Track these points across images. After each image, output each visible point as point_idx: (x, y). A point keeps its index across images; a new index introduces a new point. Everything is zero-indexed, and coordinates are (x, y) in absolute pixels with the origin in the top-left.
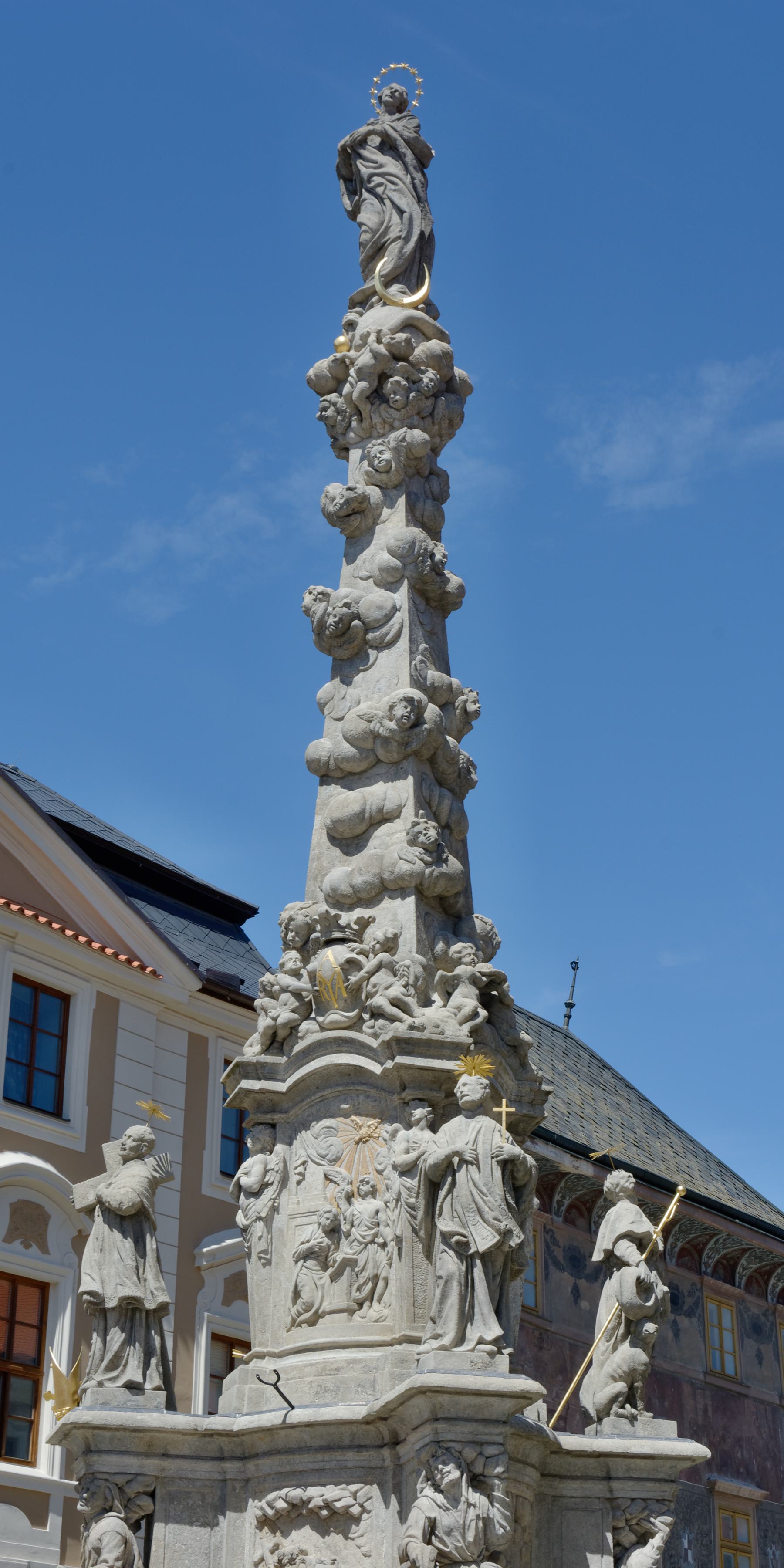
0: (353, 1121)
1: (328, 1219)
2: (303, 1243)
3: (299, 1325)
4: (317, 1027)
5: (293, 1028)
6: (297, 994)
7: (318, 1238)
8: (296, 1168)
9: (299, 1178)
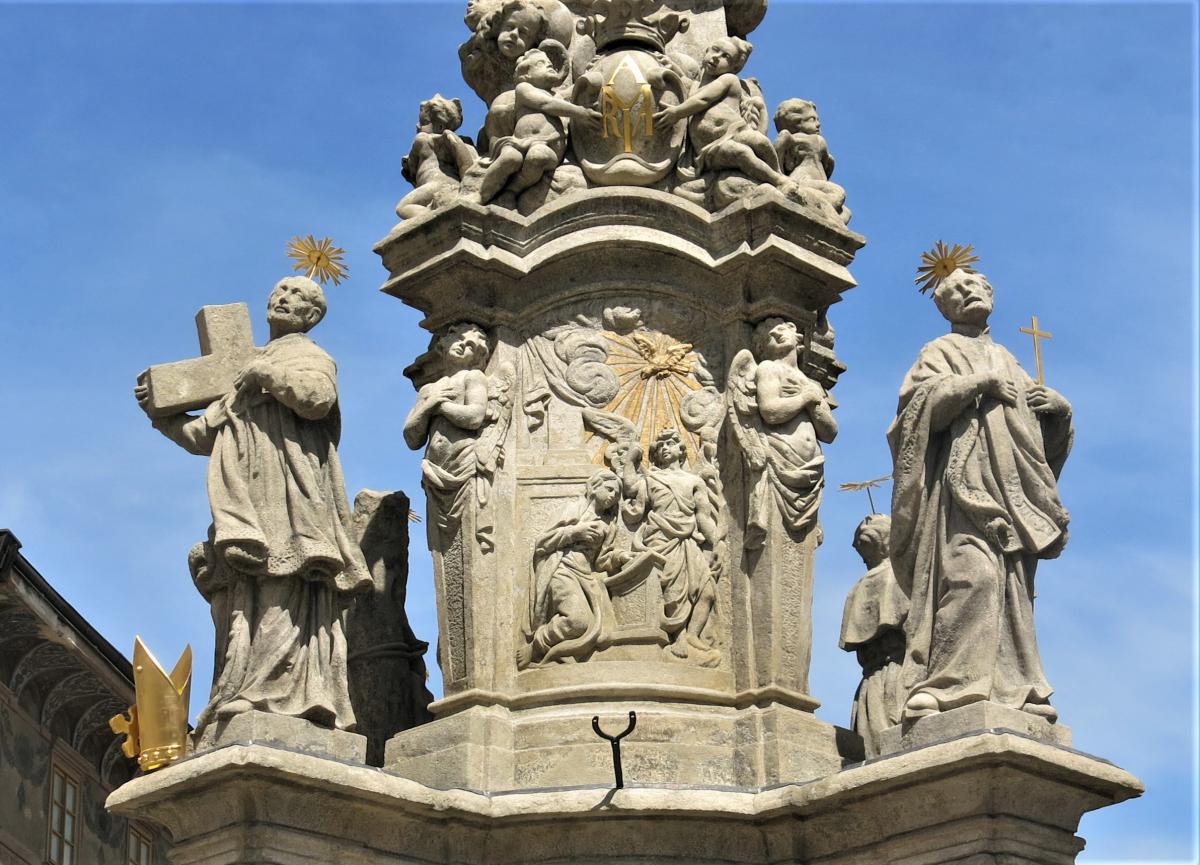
0: (637, 341)
1: (611, 489)
2: (562, 524)
3: (558, 658)
4: (582, 180)
5: (546, 170)
6: (553, 117)
7: (587, 519)
8: (529, 404)
9: (534, 421)
